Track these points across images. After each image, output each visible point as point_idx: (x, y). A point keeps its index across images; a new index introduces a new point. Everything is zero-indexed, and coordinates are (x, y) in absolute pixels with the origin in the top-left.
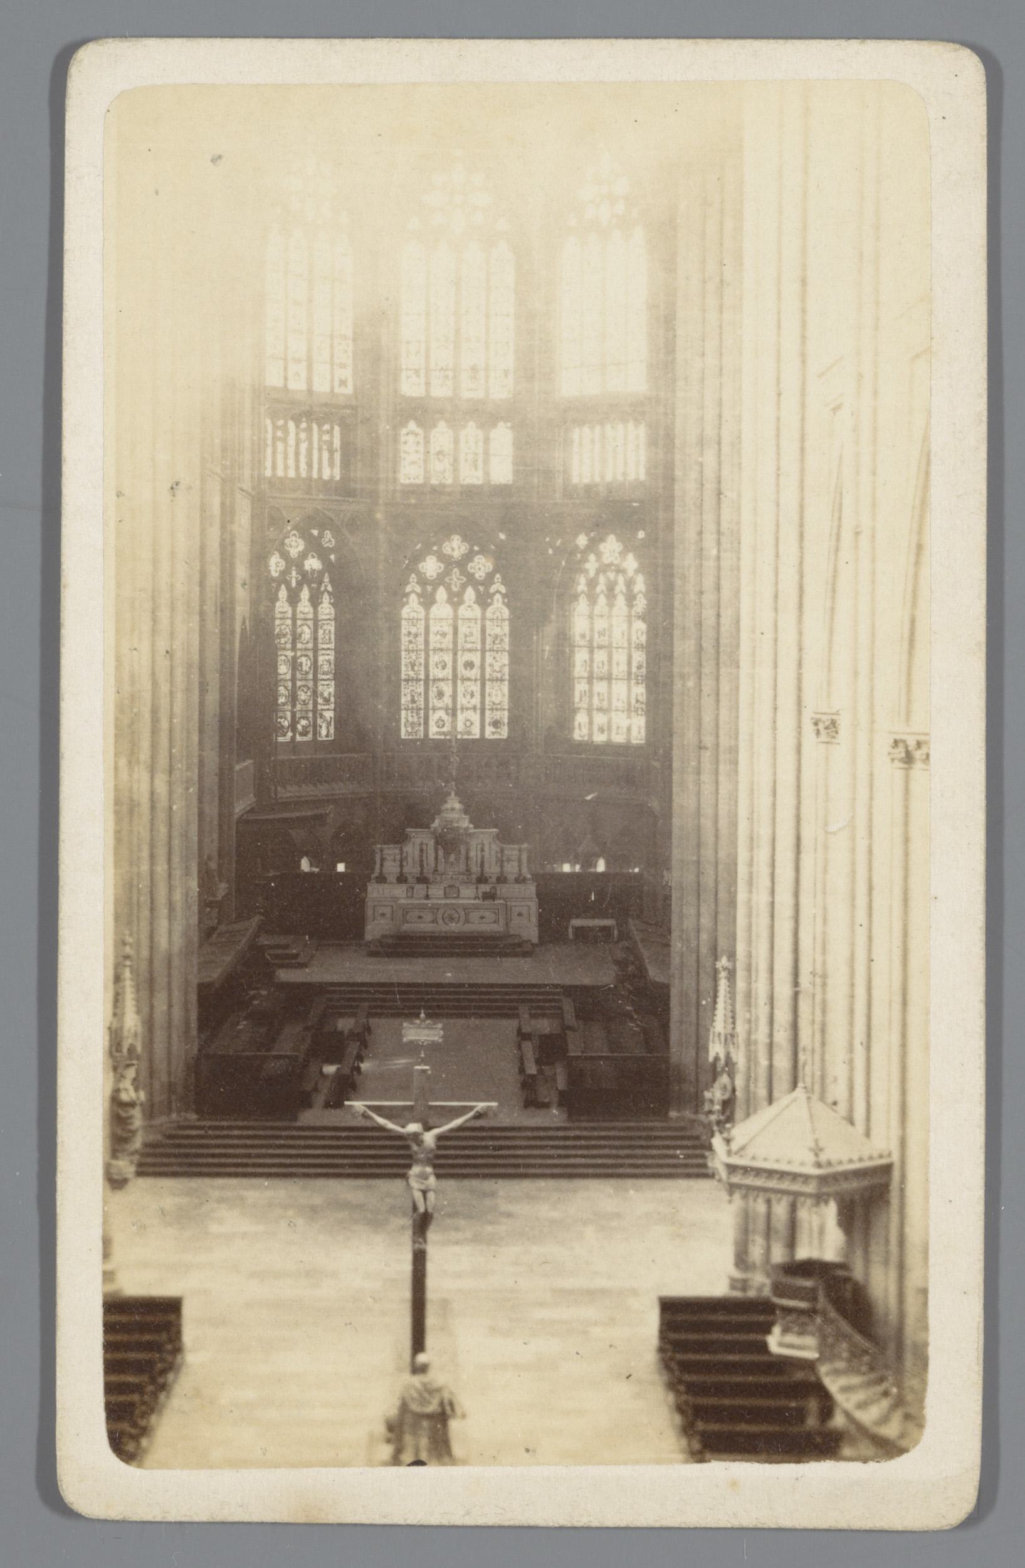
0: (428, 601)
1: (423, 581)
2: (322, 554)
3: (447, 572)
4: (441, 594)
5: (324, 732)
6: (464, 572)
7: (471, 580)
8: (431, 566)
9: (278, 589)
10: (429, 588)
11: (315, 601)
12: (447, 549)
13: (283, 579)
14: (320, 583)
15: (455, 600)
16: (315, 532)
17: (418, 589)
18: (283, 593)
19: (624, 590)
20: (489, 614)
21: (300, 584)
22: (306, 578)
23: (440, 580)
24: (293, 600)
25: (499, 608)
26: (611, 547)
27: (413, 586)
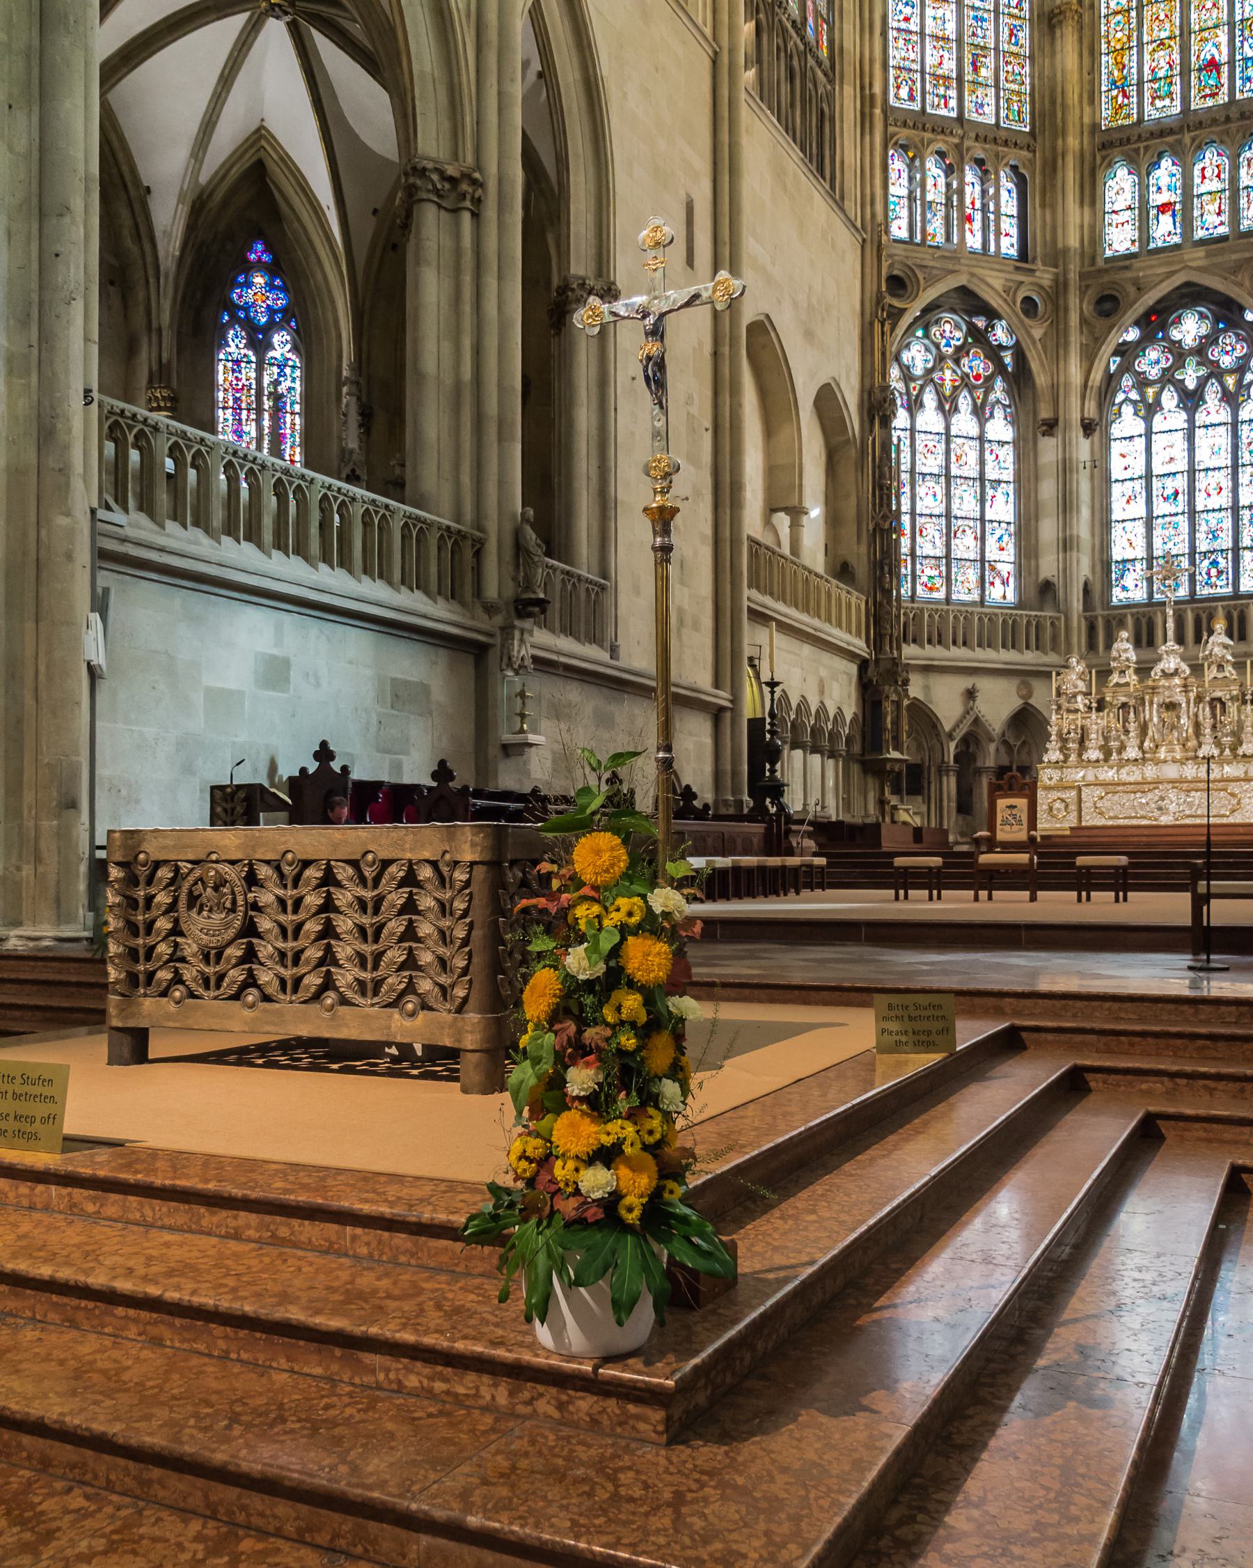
0: (1150, 410)
1: (1142, 383)
2: (993, 353)
4: (1169, 399)
6: (1203, 361)
7: (1216, 372)
8: (1152, 361)
11: (981, 412)
12: (1175, 334)
14: (989, 389)
15: (1191, 400)
16: (980, 322)
17: (1134, 395)
18: (929, 399)
23: (1167, 378)
24: (947, 407)
27: (1127, 389)
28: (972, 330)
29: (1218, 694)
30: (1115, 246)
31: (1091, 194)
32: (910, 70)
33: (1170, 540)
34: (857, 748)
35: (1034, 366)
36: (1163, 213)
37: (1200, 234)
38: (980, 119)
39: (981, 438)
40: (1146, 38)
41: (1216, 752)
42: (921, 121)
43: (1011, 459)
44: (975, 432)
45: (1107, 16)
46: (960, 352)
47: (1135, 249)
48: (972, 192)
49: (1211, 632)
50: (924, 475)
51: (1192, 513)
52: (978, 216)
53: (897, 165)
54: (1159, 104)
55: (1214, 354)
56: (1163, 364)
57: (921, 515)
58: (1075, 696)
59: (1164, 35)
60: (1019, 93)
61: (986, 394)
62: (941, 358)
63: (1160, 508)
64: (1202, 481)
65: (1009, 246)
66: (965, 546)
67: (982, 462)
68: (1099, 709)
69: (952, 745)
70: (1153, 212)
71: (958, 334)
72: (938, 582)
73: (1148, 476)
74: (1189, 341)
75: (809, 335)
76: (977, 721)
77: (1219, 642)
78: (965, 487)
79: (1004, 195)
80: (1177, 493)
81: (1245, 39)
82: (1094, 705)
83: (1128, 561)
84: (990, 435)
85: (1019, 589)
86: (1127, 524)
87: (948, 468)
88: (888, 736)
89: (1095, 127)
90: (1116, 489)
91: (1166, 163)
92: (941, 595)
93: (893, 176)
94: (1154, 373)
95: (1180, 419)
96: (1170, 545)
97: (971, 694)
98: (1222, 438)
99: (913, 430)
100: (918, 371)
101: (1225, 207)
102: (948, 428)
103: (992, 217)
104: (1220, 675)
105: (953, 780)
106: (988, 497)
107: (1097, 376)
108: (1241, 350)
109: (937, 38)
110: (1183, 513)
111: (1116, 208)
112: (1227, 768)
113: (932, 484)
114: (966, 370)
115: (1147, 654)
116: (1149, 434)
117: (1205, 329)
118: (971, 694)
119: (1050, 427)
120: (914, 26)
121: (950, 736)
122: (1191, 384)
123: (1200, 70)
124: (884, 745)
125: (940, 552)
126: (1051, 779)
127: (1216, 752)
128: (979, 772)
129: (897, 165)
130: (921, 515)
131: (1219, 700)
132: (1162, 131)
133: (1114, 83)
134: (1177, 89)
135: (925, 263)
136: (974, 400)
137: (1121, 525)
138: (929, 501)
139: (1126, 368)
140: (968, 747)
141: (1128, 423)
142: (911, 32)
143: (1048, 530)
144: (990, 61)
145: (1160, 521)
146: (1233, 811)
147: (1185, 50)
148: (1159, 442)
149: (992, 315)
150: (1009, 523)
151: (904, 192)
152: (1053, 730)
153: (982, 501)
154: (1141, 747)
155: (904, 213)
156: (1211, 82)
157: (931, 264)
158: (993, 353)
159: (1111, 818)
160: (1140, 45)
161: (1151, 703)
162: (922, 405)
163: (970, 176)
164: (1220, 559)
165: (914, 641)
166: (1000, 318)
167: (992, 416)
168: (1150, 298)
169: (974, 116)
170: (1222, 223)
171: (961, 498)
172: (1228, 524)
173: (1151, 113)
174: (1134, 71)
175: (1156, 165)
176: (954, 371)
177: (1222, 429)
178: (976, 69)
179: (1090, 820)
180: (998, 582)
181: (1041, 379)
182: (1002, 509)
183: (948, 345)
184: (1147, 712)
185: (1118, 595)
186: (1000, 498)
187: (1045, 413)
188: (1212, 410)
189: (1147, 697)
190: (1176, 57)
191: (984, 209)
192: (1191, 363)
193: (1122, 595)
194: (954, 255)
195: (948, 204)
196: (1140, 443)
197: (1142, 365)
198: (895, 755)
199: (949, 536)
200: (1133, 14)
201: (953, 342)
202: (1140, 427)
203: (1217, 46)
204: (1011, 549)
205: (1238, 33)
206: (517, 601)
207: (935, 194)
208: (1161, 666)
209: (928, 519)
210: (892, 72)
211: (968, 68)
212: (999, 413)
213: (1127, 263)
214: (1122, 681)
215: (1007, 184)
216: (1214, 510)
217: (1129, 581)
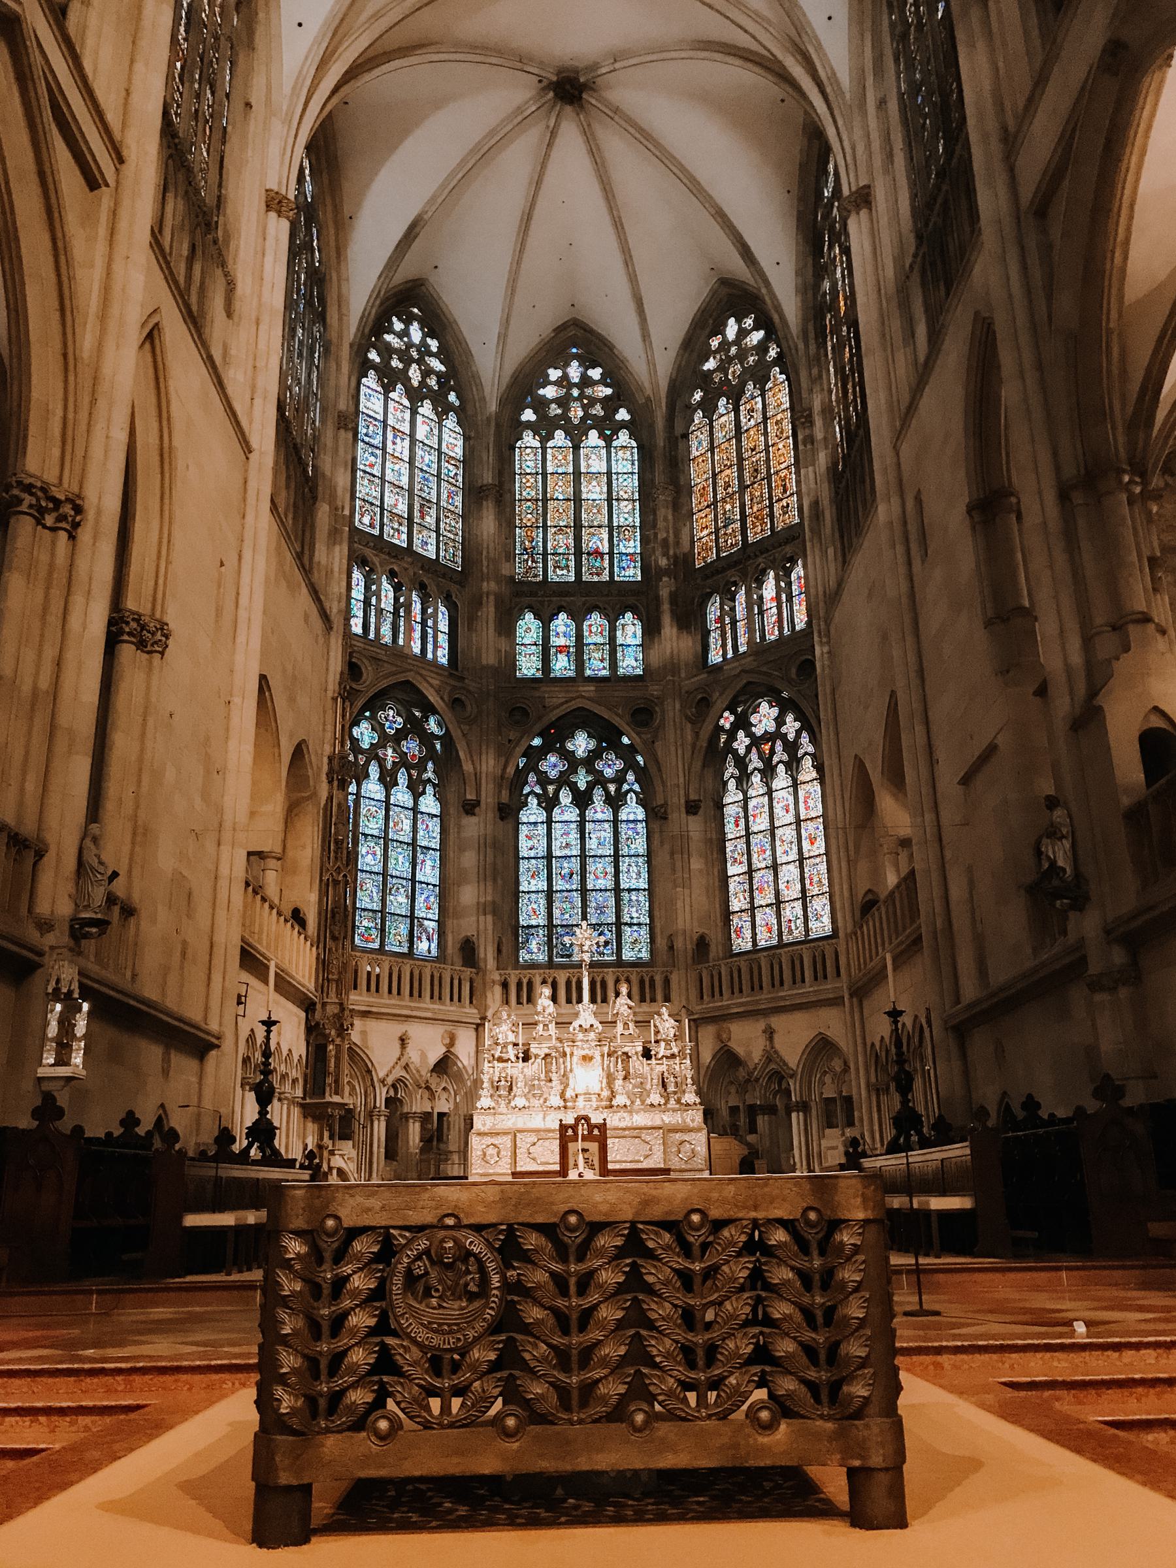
0: (549, 804)
1: (543, 780)
2: (426, 739)
3: (573, 769)
4: (565, 797)
5: (422, 947)
7: (599, 780)
8: (552, 765)
9: (367, 763)
10: (551, 788)
11: (416, 789)
12: (570, 746)
13: (373, 753)
15: (582, 800)
16: (417, 714)
17: (538, 790)
18: (374, 771)
19: (785, 757)
20: (623, 816)
22: (403, 761)
23: (564, 780)
25: (633, 810)
26: (764, 718)
28: (409, 719)
29: (626, 1049)
30: (525, 672)
31: (507, 629)
32: (372, 504)
33: (567, 911)
34: (299, 1092)
35: (462, 754)
36: (561, 652)
37: (588, 673)
38: (425, 553)
39: (415, 810)
40: (549, 524)
41: (628, 1103)
42: (379, 544)
43: (438, 829)
44: (410, 804)
45: (520, 500)
46: (400, 736)
47: (539, 675)
48: (417, 608)
49: (617, 994)
50: (366, 835)
51: (584, 891)
52: (418, 628)
53: (357, 575)
54: (559, 572)
55: (599, 765)
56: (561, 768)
57: (362, 871)
58: (505, 1046)
59: (562, 524)
60: (454, 540)
61: (420, 775)
62: (384, 737)
63: (559, 884)
64: (592, 866)
65: (443, 656)
66: (399, 902)
68: (526, 1059)
69: (384, 1090)
70: (553, 650)
71: (400, 720)
72: (374, 932)
73: (549, 857)
74: (581, 753)
75: (292, 699)
76: (406, 1067)
77: (622, 1005)
78: (400, 850)
79: (440, 615)
80: (571, 875)
81: (620, 540)
82: (521, 1055)
83: (532, 927)
84: (422, 808)
85: (441, 946)
86: (533, 896)
87: (386, 831)
88: (330, 1080)
89: (512, 578)
90: (523, 865)
91: (562, 616)
92: (376, 945)
93: (354, 582)
94: (553, 774)
95: (572, 814)
96: (567, 916)
97: (403, 1041)
98: (607, 833)
99: (358, 795)
100: (365, 745)
101: (607, 656)
102: (388, 796)
103: (429, 630)
104: (626, 1033)
105: (383, 1124)
106: (419, 861)
107: (511, 770)
108: (619, 765)
110: (576, 890)
111: (526, 641)
112: (635, 1117)
113: (372, 844)
114: (405, 750)
115: (566, 1009)
116: (549, 822)
117: (592, 744)
118: (403, 1041)
119: (470, 808)
120: (376, 471)
121: (383, 1081)
122: (582, 786)
123: (589, 554)
124: (328, 1089)
125: (376, 906)
126: (484, 1125)
127: (628, 1103)
128: (406, 1117)
130: (362, 871)
131: (626, 1054)
132: (562, 589)
133: (525, 549)
134: (572, 564)
135: (380, 657)
136: (410, 776)
137: (527, 896)
138: (369, 859)
139: (532, 767)
140: (396, 1092)
141: (532, 813)
142: (374, 476)
143: (468, 895)
144: (433, 512)
145: (558, 895)
146: (646, 1157)
147: (578, 539)
148: (558, 829)
149: (429, 709)
150: (434, 886)
151: (362, 597)
152: (485, 1078)
153: (414, 865)
154: (562, 1095)
155: (360, 614)
156: (597, 564)
157: (385, 658)
158: (426, 739)
159: (542, 1164)
160: (545, 527)
161: (572, 1054)
162: (367, 776)
163: (415, 597)
164: (606, 932)
165: (355, 988)
166: (434, 711)
167: (424, 793)
168: (553, 716)
169: (420, 551)
170: (604, 668)
171: (396, 859)
172: (612, 902)
173: (552, 576)
174: (540, 544)
175: (554, 616)
176: (394, 751)
177: (606, 825)
178: (422, 518)
179: (525, 1165)
180: (424, 937)
181: (467, 767)
182: (429, 872)
183: (390, 727)
184: (568, 1064)
185: (524, 956)
186: (429, 863)
187: (470, 796)
188: (599, 809)
189: (568, 1050)
190: (571, 542)
191: (424, 623)
192: (582, 772)
193: (527, 957)
194: (397, 654)
195: (396, 614)
196: (542, 830)
197: (544, 766)
198: (336, 1099)
200: (540, 504)
201: (395, 726)
202: (543, 816)
203: (601, 540)
204: (436, 906)
205: (615, 534)
206: (74, 919)
207: (387, 603)
208: (576, 1024)
209: (368, 876)
210: (358, 502)
211: (417, 514)
212: (429, 789)
213: (534, 685)
214: (546, 1034)
215: (442, 609)
216: (601, 890)
217: (533, 946)
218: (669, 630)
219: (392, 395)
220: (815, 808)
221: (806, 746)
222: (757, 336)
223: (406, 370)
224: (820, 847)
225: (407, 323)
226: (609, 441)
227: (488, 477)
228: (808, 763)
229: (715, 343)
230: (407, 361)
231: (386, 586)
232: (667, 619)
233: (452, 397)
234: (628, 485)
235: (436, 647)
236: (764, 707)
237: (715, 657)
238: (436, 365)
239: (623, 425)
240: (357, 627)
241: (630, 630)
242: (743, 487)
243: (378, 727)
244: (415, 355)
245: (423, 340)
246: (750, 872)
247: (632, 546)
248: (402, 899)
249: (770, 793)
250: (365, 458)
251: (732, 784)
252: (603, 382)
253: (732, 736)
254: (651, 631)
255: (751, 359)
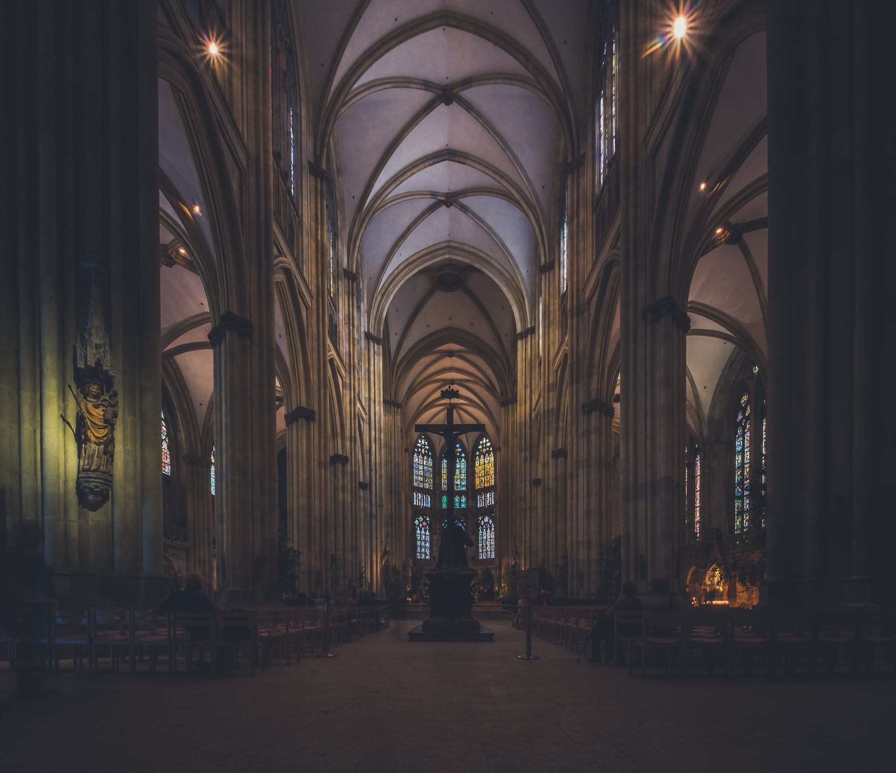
11: (425, 531)
13: (418, 525)
14: (426, 527)
21: (422, 527)
22: (423, 526)
24: (421, 530)
26: (486, 519)
28: (424, 518)
53: (415, 494)
62: (420, 522)
65: (429, 506)
67: (425, 538)
109: (420, 475)
119: (435, 534)
129: (415, 494)
158: (427, 521)
182: (428, 545)
195: (421, 500)
199: (421, 549)
218: (470, 501)
219: (420, 457)
220: (493, 536)
221: (493, 525)
222: (489, 444)
223: (421, 451)
224: (493, 543)
225: (421, 440)
226: (460, 461)
227: (437, 470)
228: (493, 529)
229: (481, 443)
230: (421, 449)
231: (419, 494)
232: (470, 498)
233: (430, 454)
234: (464, 471)
235: (428, 504)
236: (487, 517)
237: (479, 506)
238: (427, 447)
239: (463, 457)
240: (415, 504)
241: (464, 499)
242: (485, 475)
243: (419, 521)
244: (423, 447)
245: (425, 443)
246: (483, 545)
247: (464, 483)
248: (424, 550)
249: (486, 532)
250: (415, 472)
251: (480, 530)
252: (459, 448)
253: (481, 521)
254: (467, 502)
255: (488, 449)
